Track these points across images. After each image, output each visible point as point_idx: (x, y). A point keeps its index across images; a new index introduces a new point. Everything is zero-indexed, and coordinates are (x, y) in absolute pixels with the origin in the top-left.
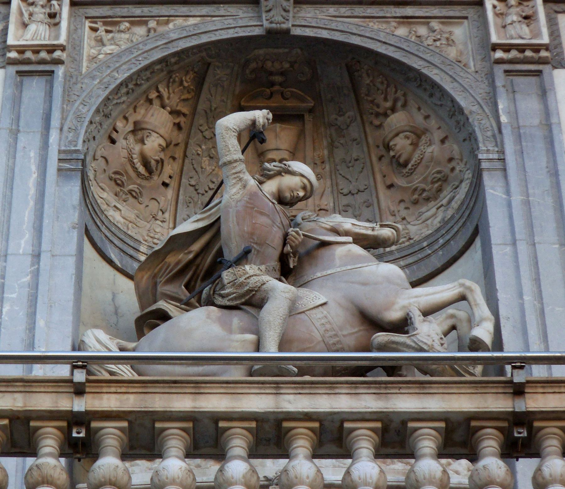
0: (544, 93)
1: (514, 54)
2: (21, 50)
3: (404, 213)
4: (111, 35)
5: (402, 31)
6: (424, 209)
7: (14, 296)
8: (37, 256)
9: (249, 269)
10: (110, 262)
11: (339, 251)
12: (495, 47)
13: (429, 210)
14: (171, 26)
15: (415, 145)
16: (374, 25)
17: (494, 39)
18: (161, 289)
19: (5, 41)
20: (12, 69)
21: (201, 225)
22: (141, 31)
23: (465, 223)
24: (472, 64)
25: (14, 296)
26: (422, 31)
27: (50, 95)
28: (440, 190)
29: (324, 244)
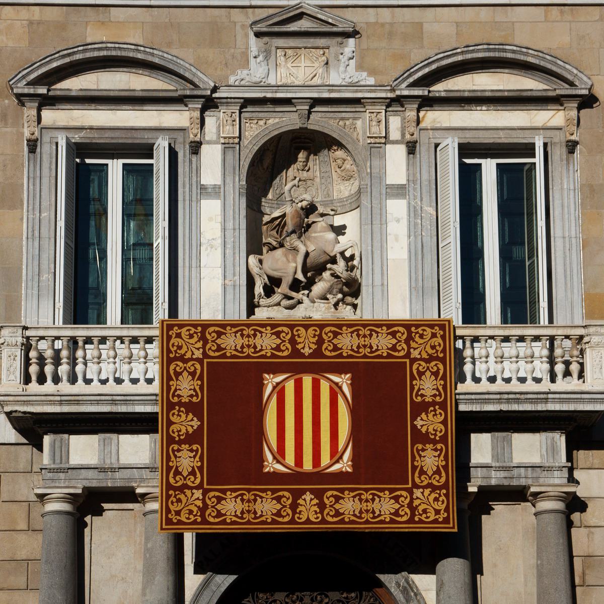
0: (383, 157)
1: (373, 140)
2: (225, 138)
3: (339, 181)
4: (252, 125)
5: (341, 123)
6: (345, 182)
7: (229, 246)
8: (234, 229)
9: (294, 236)
10: (254, 210)
11: (319, 224)
12: (368, 137)
13: (347, 183)
14: (270, 121)
15: (343, 163)
16: (331, 122)
17: (368, 135)
18: (269, 233)
19: (220, 134)
20: (224, 146)
21: (280, 214)
22: (261, 123)
23: (356, 200)
24: (361, 141)
25: (229, 246)
26: (348, 123)
27: (234, 156)
28: (350, 179)
29: (314, 222)
